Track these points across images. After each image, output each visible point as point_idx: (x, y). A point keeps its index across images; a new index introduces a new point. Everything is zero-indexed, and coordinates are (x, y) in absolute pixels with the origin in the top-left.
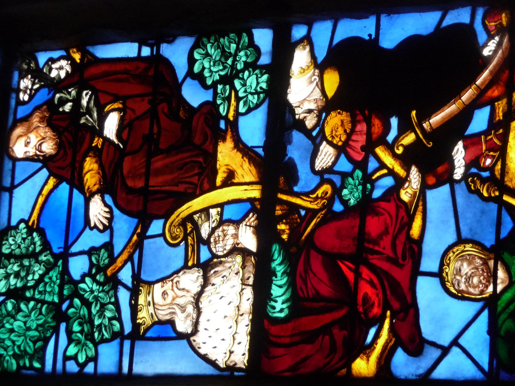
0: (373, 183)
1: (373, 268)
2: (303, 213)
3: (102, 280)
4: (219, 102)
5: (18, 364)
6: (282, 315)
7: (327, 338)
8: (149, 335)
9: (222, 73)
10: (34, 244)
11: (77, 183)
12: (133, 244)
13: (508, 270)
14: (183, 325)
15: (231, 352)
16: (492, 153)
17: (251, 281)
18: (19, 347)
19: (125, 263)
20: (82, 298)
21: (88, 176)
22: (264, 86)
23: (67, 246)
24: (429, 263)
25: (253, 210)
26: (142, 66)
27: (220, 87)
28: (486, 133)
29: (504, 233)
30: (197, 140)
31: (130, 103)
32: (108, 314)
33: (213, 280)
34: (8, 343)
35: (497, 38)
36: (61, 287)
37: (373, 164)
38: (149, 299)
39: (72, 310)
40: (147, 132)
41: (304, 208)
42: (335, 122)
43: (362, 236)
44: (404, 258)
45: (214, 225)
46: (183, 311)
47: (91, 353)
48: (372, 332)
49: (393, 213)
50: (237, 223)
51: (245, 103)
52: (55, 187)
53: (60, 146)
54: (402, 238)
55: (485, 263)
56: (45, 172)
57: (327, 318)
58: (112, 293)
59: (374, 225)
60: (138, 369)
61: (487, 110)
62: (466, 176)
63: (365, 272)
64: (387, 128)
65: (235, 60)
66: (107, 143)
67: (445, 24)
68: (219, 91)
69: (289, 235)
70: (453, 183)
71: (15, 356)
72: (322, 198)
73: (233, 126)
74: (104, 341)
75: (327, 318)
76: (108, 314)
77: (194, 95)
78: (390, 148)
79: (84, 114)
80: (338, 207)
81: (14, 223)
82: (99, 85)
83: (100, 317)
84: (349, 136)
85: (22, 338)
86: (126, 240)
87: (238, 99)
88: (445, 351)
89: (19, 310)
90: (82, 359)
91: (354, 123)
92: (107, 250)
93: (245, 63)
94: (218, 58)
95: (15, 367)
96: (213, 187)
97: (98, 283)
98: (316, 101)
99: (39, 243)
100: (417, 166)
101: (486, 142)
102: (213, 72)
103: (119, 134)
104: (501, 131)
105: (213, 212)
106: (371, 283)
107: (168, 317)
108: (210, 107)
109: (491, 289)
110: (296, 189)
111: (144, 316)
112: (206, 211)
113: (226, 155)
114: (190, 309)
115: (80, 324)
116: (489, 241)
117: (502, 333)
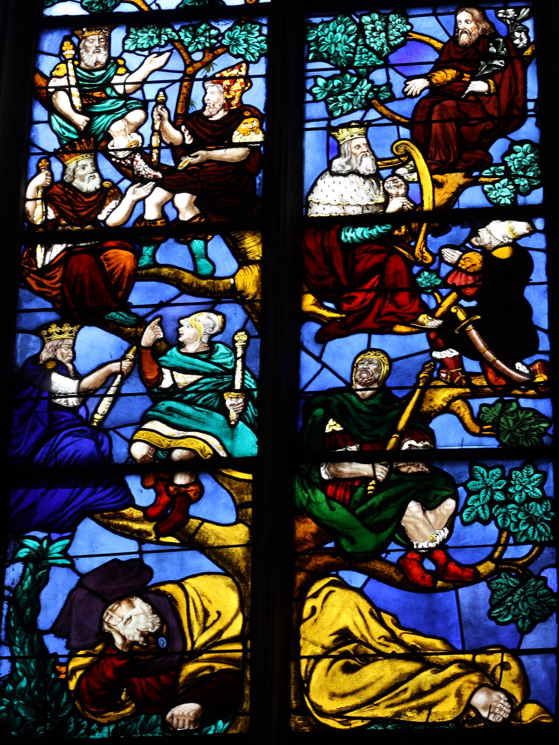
0: (432, 294)
1: (374, 301)
2: (413, 244)
3: (369, 97)
4: (492, 169)
5: (311, 41)
6: (343, 238)
7: (327, 273)
8: (331, 139)
9: (512, 168)
10: (395, 40)
11: (438, 66)
13: (371, 397)
14: (337, 164)
15: (318, 203)
16: (449, 377)
17: (366, 211)
18: (324, 40)
19: (380, 113)
20: (357, 83)
21: (442, 73)
22: (503, 202)
23: (393, 66)
24: (377, 341)
25: (416, 206)
26: (520, 104)
27: (502, 168)
28: (463, 371)
29: (395, 392)
30: (466, 156)
31: (494, 98)
32: (345, 106)
34: (326, 32)
35: (527, 372)
36: (365, 66)
37: (444, 291)
38: (356, 136)
39: (348, 76)
40: (472, 116)
41: (416, 244)
42: (475, 259)
43: (397, 290)
44: (381, 322)
45: (405, 177)
46: (346, 163)
47: (319, 97)
48: (331, 305)
49: (412, 310)
50: (406, 195)
51: (491, 189)
53: (465, 47)
54: (394, 319)
55: (376, 381)
56: (446, 39)
57: (340, 271)
58: (360, 105)
59: (403, 297)
60: (308, 134)
61: (479, 370)
62: (435, 360)
63: (371, 295)
64: (469, 299)
65: (521, 176)
66: (465, 85)
67: (539, 332)
68: (500, 168)
69: (397, 235)
70: (430, 351)
71: (318, 37)
72: (422, 257)
73: (475, 182)
74: (327, 104)
75: (340, 271)
76: (345, 106)
77: (497, 149)
78: (455, 303)
79: (487, 64)
80: (416, 269)
81: (411, 20)
82: (507, 72)
83: (344, 99)
84: (465, 271)
85: (330, 41)
86: (396, 111)
87: (493, 183)
88: (318, 359)
89: (349, 35)
90: (315, 90)
91: (474, 274)
92: (390, 97)
93: (519, 185)
94: (523, 163)
95: (310, 39)
96: (432, 173)
97: (367, 94)
98: (491, 243)
99: (396, 42)
100: (442, 324)
101: (457, 372)
102: (513, 162)
103: (472, 93)
104: (464, 382)
105: (414, 176)
106: (364, 300)
107: (342, 152)
108: (488, 162)
109: (359, 387)
110: (429, 236)
111: (344, 134)
112: (415, 170)
113: (454, 179)
114: (348, 168)
115: (339, 85)
116: (390, 383)
117: (330, 398)
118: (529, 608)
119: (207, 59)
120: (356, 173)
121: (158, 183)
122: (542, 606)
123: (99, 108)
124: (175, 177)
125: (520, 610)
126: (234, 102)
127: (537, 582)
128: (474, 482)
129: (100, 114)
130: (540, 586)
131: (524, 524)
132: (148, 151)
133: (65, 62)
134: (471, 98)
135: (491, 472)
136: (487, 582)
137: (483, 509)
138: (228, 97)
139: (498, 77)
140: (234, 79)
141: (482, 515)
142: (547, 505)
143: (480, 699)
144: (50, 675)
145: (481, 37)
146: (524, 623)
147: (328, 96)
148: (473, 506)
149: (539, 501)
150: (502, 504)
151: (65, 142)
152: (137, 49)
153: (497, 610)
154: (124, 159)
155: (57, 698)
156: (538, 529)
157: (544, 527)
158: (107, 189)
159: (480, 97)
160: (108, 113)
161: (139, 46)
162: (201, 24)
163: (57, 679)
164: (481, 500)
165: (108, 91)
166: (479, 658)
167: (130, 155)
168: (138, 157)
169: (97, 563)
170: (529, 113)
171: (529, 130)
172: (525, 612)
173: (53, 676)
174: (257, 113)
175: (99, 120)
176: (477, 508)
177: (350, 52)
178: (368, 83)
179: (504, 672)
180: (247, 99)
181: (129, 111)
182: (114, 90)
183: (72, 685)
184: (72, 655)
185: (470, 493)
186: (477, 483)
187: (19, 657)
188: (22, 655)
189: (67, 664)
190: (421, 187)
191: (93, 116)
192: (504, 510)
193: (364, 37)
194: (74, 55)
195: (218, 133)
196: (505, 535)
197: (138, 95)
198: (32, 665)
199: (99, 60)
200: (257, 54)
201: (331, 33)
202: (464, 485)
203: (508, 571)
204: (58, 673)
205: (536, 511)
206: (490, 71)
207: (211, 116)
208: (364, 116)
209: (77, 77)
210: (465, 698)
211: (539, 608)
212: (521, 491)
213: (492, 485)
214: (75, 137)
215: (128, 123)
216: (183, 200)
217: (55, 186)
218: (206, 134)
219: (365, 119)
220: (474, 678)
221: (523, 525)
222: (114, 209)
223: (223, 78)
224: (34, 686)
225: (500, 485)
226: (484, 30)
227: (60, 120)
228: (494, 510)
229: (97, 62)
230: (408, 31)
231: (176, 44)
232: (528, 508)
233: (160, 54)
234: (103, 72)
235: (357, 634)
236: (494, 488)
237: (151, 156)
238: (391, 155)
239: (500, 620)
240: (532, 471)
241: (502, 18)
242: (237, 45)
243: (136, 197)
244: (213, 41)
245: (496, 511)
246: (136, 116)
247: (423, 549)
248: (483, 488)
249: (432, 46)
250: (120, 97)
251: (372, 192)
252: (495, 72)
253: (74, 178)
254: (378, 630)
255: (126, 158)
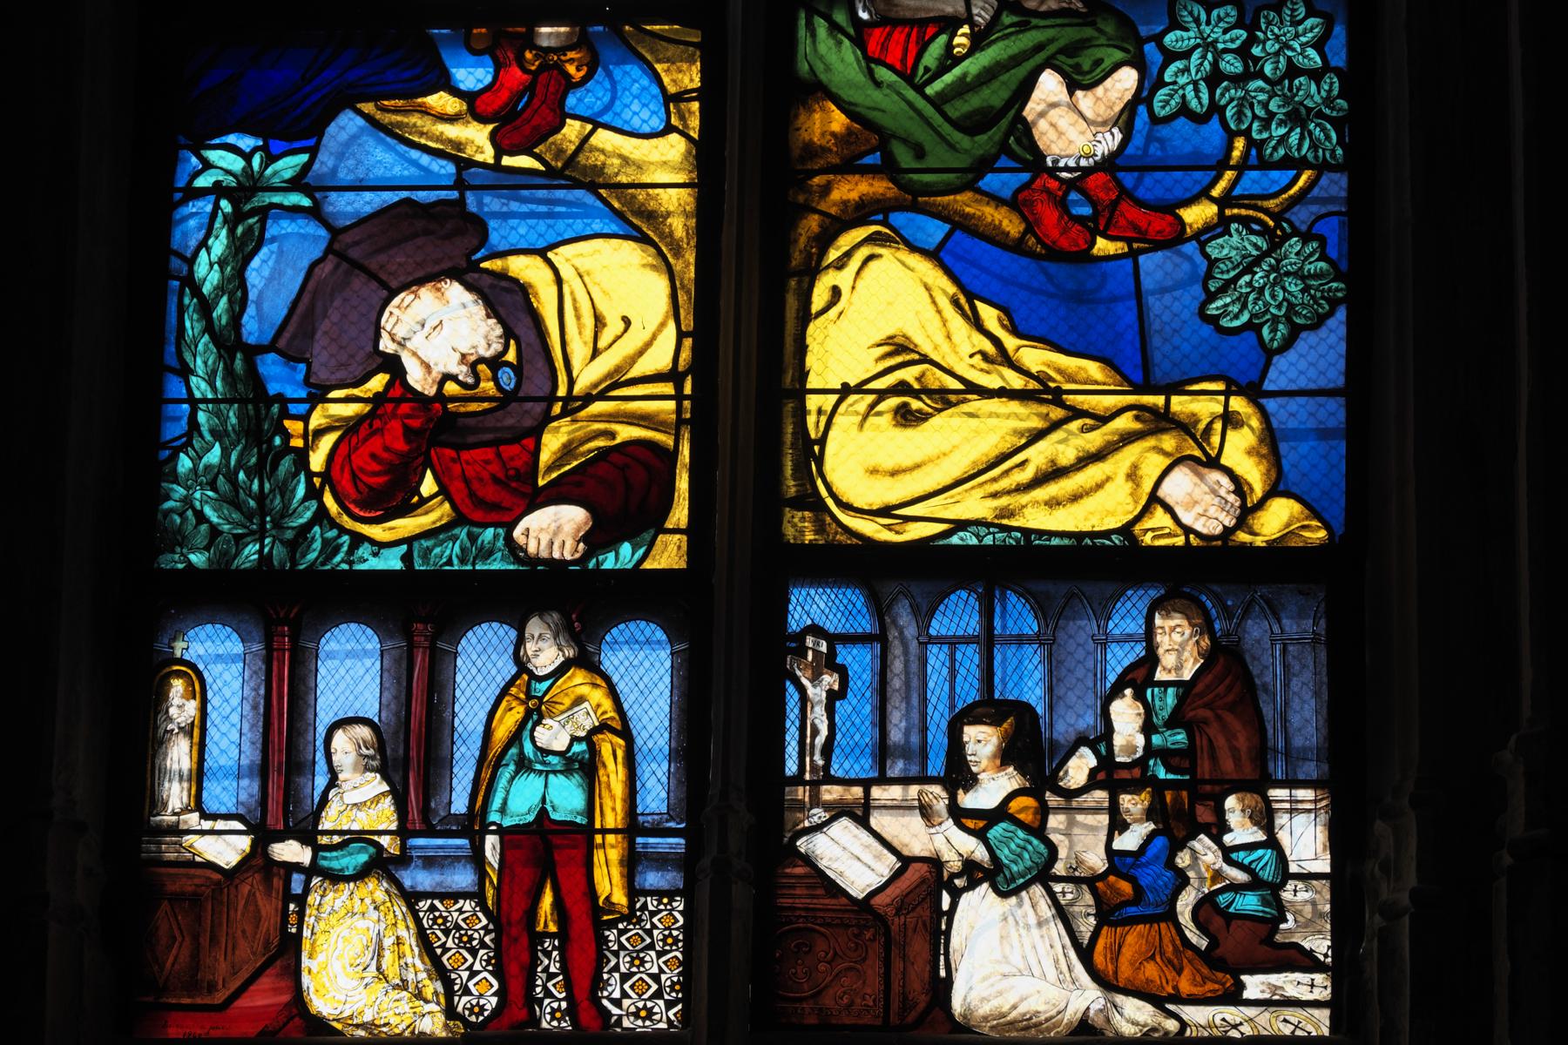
118: (1285, 299)
122: (1313, 297)
125: (1266, 304)
127: (1305, 243)
128: (1179, 33)
130: (1311, 255)
131: (1281, 123)
135: (1215, 13)
136: (1199, 242)
137: (1197, 90)
141: (1194, 104)
142: (1331, 84)
143: (1180, 486)
144: (271, 439)
146: (1274, 330)
148: (1175, 83)
149: (1316, 75)
150: (1239, 80)
153: (1219, 303)
155: (285, 490)
156: (1310, 134)
157: (1323, 130)
163: (287, 449)
164: (1193, 71)
166: (1179, 404)
169: (368, 202)
172: (1279, 307)
173: (278, 441)
176: (1183, 87)
179: (1230, 434)
183: (317, 461)
184: (318, 396)
185: (1170, 56)
186: (1185, 34)
187: (205, 400)
188: (210, 396)
189: (305, 418)
192: (1240, 93)
196: (1240, 144)
198: (234, 420)
202: (1158, 39)
203: (1245, 221)
204: (287, 436)
205: (1309, 96)
210: (1147, 486)
211: (1307, 298)
212: (1277, 54)
213: (1216, 41)
220: (1169, 442)
221: (1279, 125)
224: (239, 461)
225: (1232, 41)
228: (1218, 92)
232: (1290, 89)
235: (926, 348)
236: (1221, 46)
239: (1225, 323)
240: (1302, 11)
245: (1223, 95)
247: (1067, 169)
248: (1198, 46)
254: (967, 341)
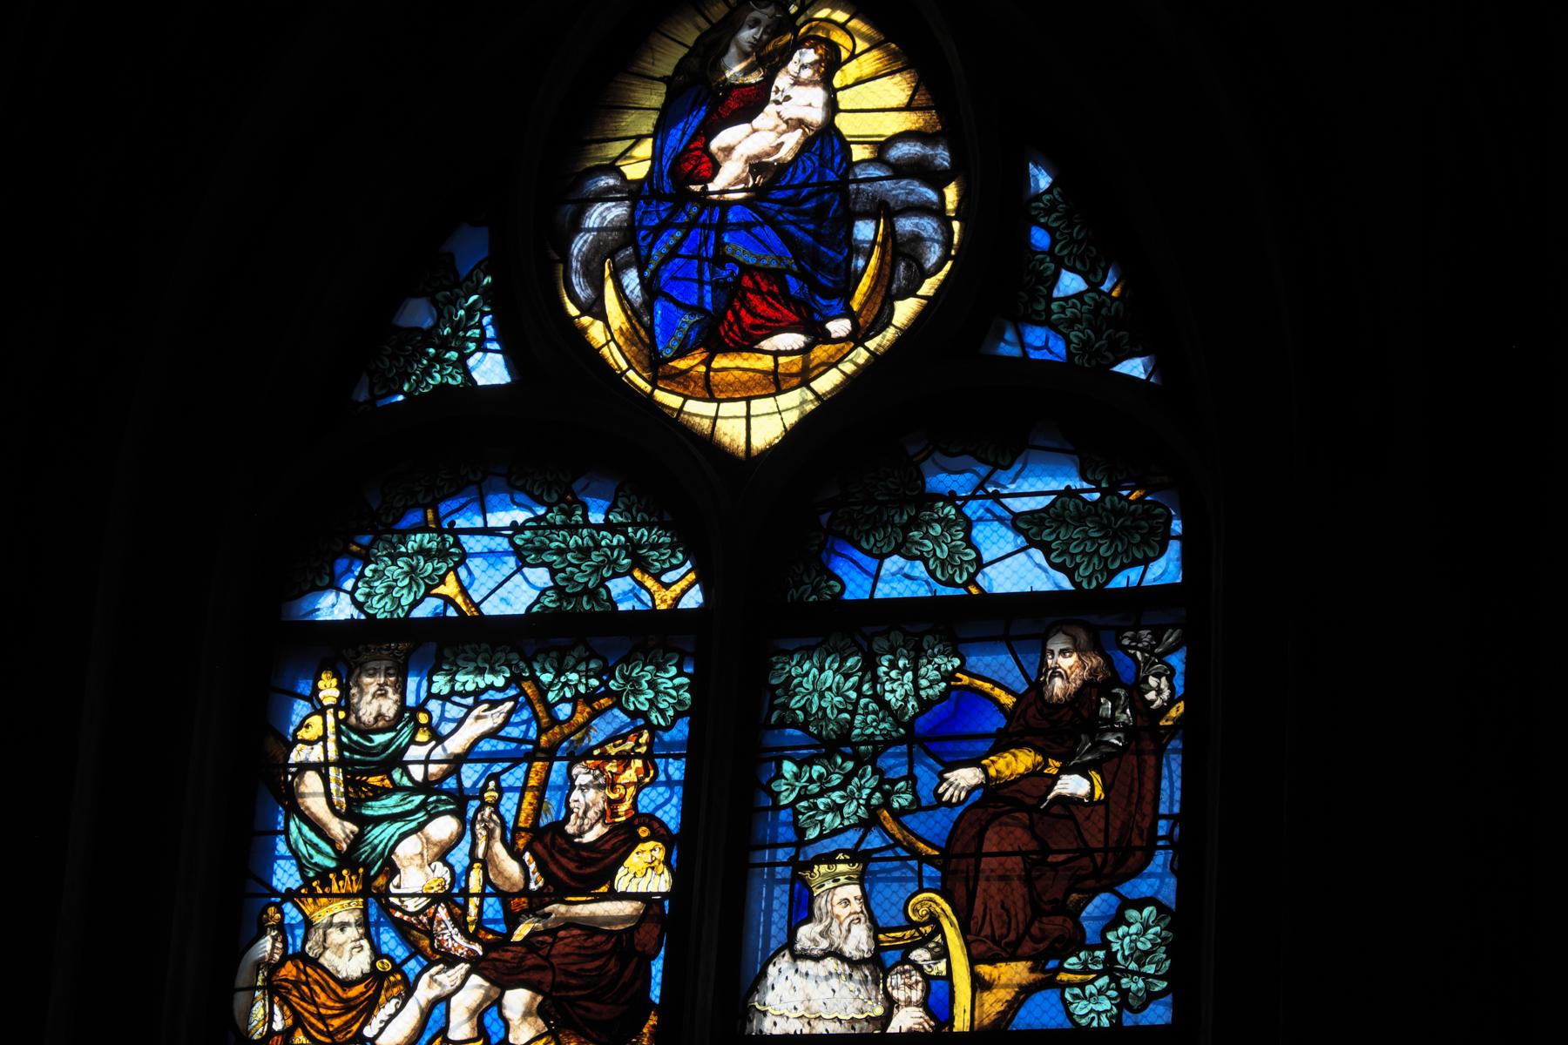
3: (874, 802)
4: (1082, 955)
9: (1119, 956)
10: (930, 687)
12: (910, 843)
20: (853, 773)
26: (1147, 823)
27: (1101, 954)
31: (1101, 810)
33: (857, 976)
46: (821, 934)
52: (1001, 706)
53: (1058, 706)
65: (1133, 973)
66: (1050, 781)
68: (1097, 953)
73: (1048, 982)
79: (1092, 740)
85: (810, 687)
86: (920, 832)
87: (1082, 985)
89: (847, 677)
94: (1140, 945)
95: (774, 682)
96: (973, 961)
97: (870, 796)
99: (931, 692)
102: (1122, 941)
103: (1060, 798)
105: (941, 967)
107: (816, 912)
112: (943, 953)
113: (1014, 973)
114: (824, 944)
115: (820, 776)
119: (579, 718)
120: (838, 954)
121: (477, 965)
123: (376, 808)
124: (508, 956)
126: (623, 808)
129: (378, 821)
132: (460, 900)
133: (321, 711)
134: (1056, 810)
138: (612, 796)
139: (1109, 766)
140: (625, 759)
145: (1086, 684)
147: (799, 798)
151: (311, 874)
152: (453, 692)
154: (416, 914)
158: (385, 975)
159: (1073, 808)
160: (393, 818)
161: (458, 687)
162: (573, 648)
165: (396, 775)
167: (428, 906)
168: (442, 913)
170: (1160, 843)
171: (1157, 879)
174: (662, 831)
175: (377, 831)
177: (845, 711)
178: (873, 774)
180: (649, 800)
181: (432, 817)
182: (407, 773)
190: (952, 986)
191: (365, 823)
193: (875, 680)
194: (339, 699)
195: (592, 869)
197: (451, 783)
199: (384, 710)
200: (671, 713)
201: (814, 671)
206: (1097, 756)
207: (581, 834)
208: (861, 840)
209: (341, 746)
214: (332, 864)
215: (428, 841)
216: (517, 1000)
217: (289, 964)
218: (567, 872)
219: (864, 846)
222: (392, 1017)
223: (606, 758)
226: (1093, 672)
227: (305, 829)
229: (380, 716)
230: (955, 670)
231: (525, 685)
233: (494, 704)
234: (390, 735)
237: (465, 908)
238: (903, 922)
241: (1130, 647)
242: (637, 692)
243: (436, 991)
244: (594, 682)
246: (443, 828)
249: (995, 701)
250: (417, 788)
251: (863, 995)
252: (1109, 756)
253: (325, 949)
255: (422, 911)
